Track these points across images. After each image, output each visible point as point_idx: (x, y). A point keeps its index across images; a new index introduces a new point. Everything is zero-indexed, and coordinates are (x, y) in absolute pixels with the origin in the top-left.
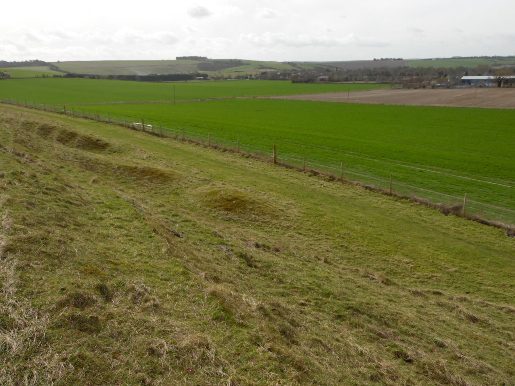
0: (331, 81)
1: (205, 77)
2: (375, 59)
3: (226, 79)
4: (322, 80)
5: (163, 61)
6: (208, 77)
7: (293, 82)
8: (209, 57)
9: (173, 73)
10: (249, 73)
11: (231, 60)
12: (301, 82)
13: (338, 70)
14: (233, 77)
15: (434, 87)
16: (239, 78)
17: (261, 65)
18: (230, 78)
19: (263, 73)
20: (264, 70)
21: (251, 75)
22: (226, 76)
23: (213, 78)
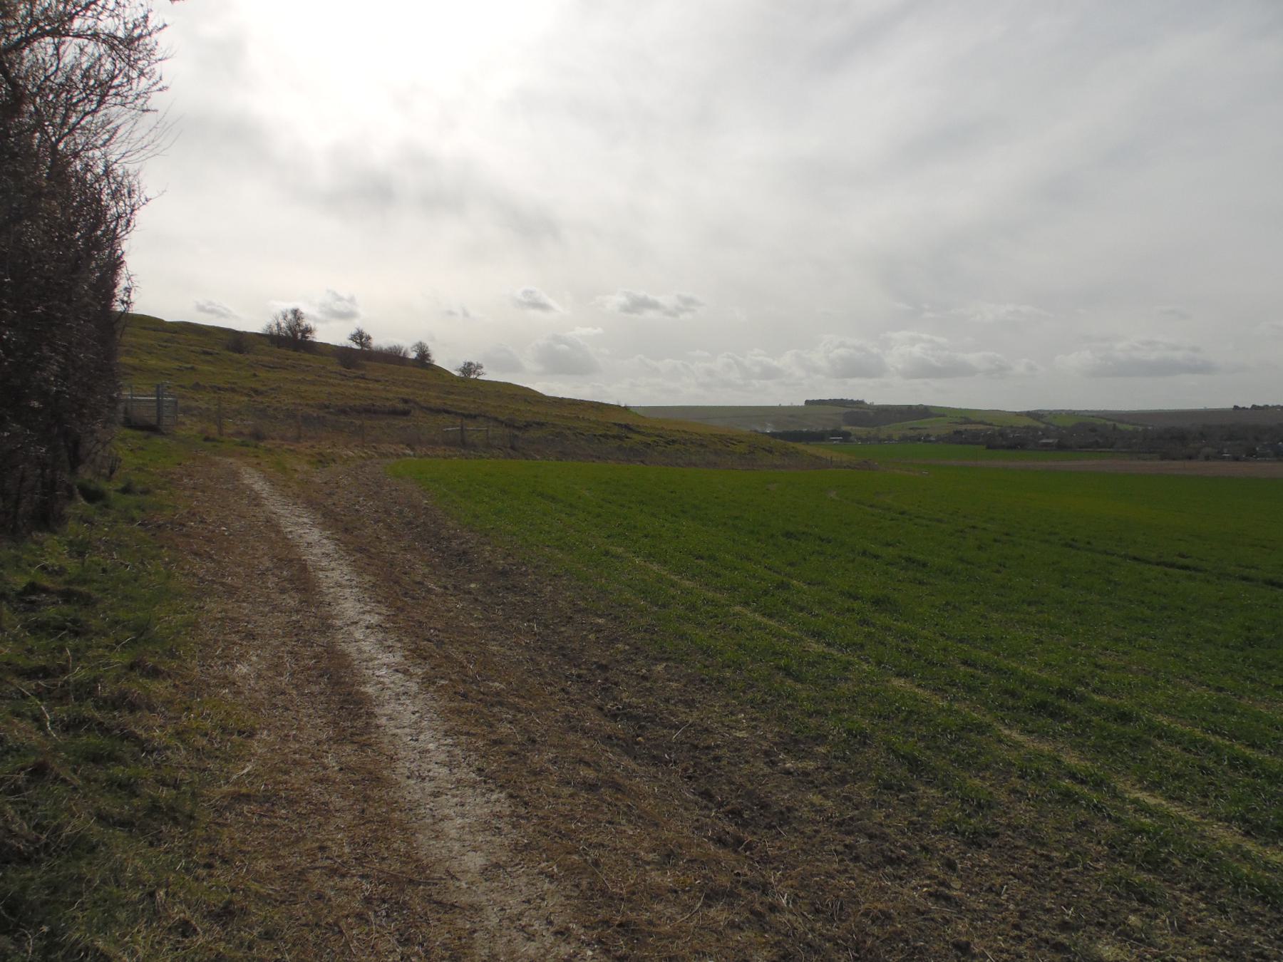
0: (1061, 447)
1: (846, 436)
2: (1236, 407)
3: (880, 441)
4: (1046, 445)
5: (780, 407)
6: (852, 438)
7: (989, 447)
8: (868, 401)
9: (793, 428)
10: (925, 432)
11: (910, 407)
12: (1003, 447)
13: (1121, 426)
14: (896, 437)
15: (1207, 458)
16: (904, 439)
17: (965, 416)
18: (890, 438)
19: (958, 433)
20: (963, 427)
21: (928, 436)
22: (882, 436)
23: (860, 439)
